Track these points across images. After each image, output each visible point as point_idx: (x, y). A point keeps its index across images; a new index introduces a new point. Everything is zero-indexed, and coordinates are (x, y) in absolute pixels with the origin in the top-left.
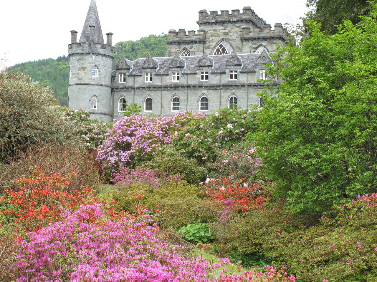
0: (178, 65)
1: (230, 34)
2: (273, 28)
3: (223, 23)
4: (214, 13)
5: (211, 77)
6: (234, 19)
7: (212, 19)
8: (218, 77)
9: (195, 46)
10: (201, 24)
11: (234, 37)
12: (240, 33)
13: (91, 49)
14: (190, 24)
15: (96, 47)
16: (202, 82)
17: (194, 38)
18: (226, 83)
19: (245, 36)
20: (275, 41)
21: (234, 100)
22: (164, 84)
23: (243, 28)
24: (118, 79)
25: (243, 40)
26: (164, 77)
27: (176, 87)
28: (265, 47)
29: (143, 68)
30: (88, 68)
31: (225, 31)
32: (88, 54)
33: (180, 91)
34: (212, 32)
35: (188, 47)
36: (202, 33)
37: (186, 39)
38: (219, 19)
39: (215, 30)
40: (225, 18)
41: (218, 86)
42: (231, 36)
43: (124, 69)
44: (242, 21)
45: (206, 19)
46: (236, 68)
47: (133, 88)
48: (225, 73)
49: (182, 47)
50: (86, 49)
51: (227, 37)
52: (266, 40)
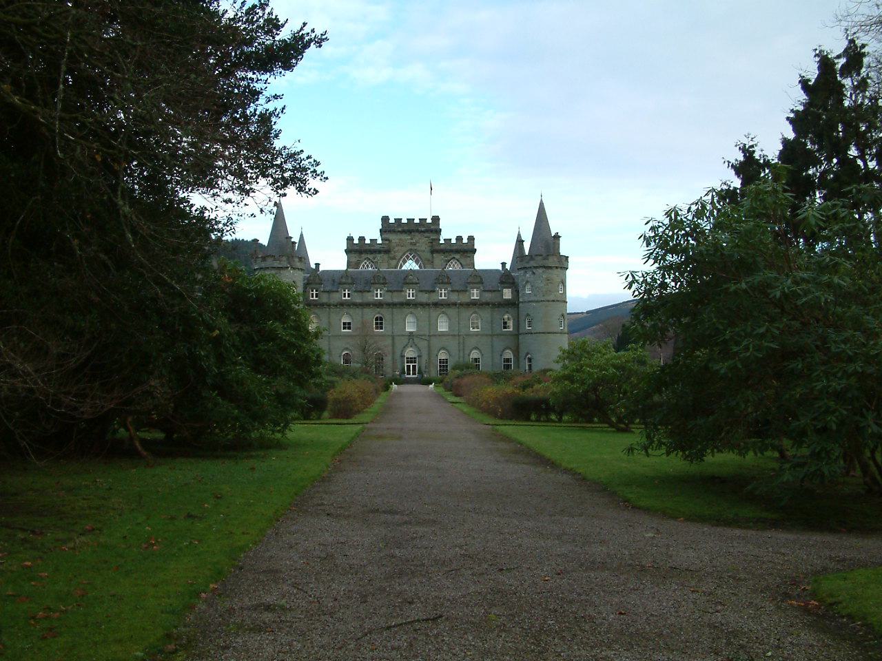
0: (381, 281)
2: (465, 241)
3: (410, 232)
4: (398, 221)
5: (420, 294)
6: (423, 229)
8: (427, 295)
9: (379, 256)
10: (385, 232)
11: (423, 248)
12: (430, 244)
14: (373, 233)
17: (377, 247)
18: (436, 301)
19: (437, 248)
20: (469, 255)
22: (365, 300)
25: (433, 252)
26: (365, 294)
27: (379, 305)
28: (458, 261)
29: (340, 284)
33: (383, 310)
34: (397, 241)
35: (370, 256)
36: (387, 242)
37: (368, 248)
38: (406, 228)
39: (400, 239)
40: (413, 228)
41: (428, 305)
43: (316, 284)
44: (432, 231)
45: (387, 227)
46: (446, 286)
47: (329, 305)
48: (434, 291)
49: (364, 256)
50: (285, 264)
52: (459, 253)
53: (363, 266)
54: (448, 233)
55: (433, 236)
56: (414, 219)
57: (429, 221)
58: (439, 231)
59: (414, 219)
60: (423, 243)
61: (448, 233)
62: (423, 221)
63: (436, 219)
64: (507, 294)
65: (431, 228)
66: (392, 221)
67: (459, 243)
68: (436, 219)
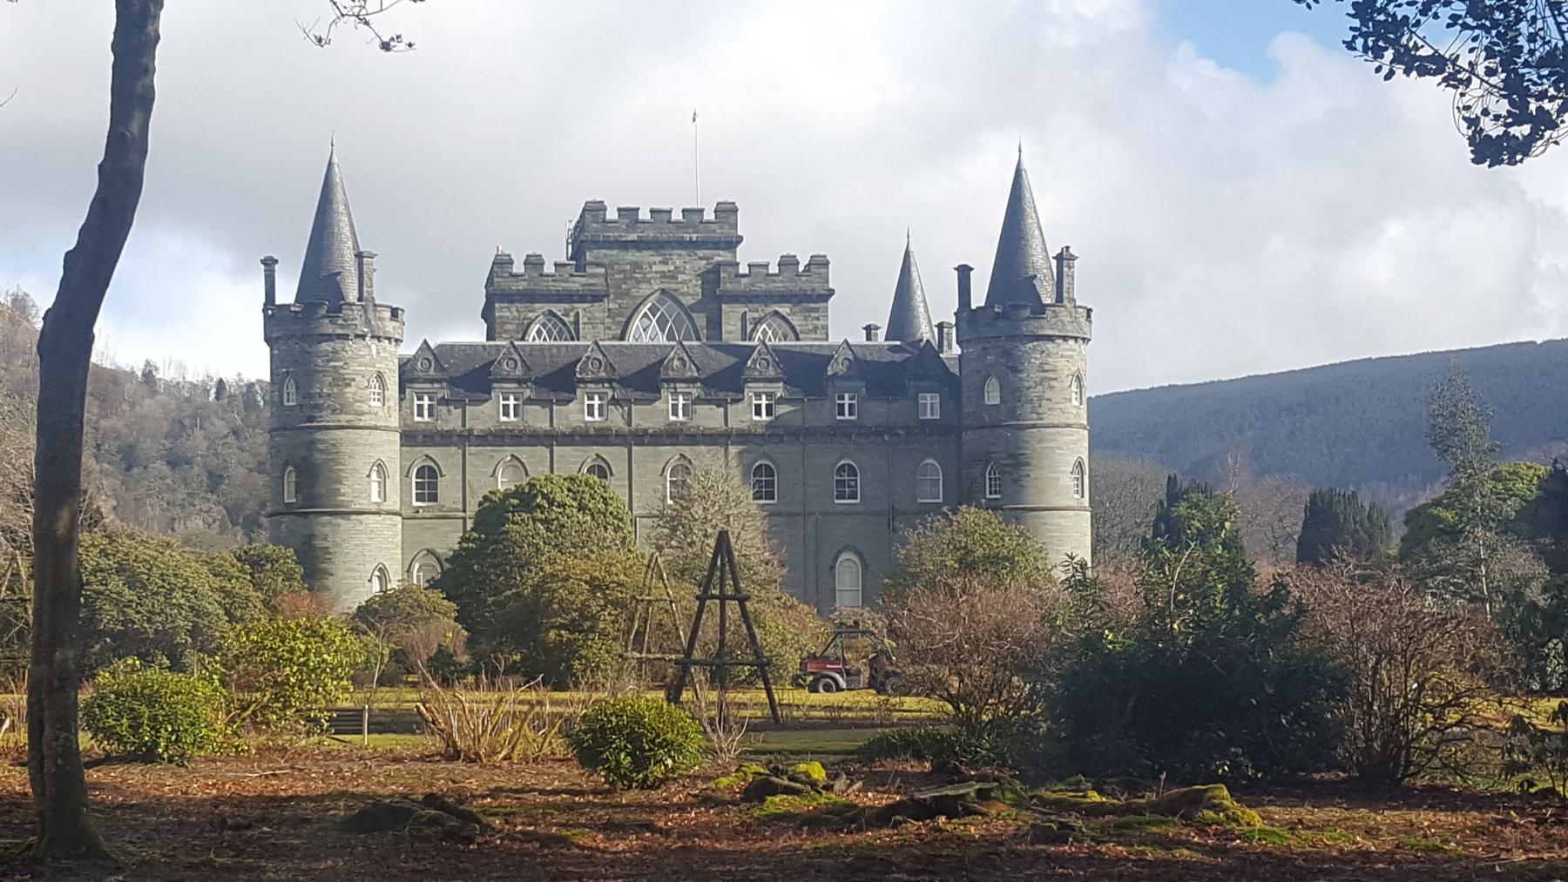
1: (681, 277)
3: (658, 245)
4: (629, 213)
7: (627, 231)
13: (368, 322)
15: (381, 319)
16: (675, 423)
18: (744, 426)
21: (685, 467)
22: (560, 425)
23: (719, 264)
24: (411, 407)
27: (602, 437)
30: (358, 378)
31: (665, 268)
32: (363, 337)
36: (602, 270)
42: (684, 282)
44: (717, 245)
51: (674, 286)
53: (539, 332)
54: (760, 246)
55: (721, 256)
56: (670, 212)
57: (709, 215)
58: (732, 243)
59: (670, 212)
60: (688, 270)
61: (760, 246)
62: (695, 217)
63: (727, 212)
64: (930, 405)
65: (714, 232)
66: (612, 214)
67: (788, 273)
68: (727, 212)
